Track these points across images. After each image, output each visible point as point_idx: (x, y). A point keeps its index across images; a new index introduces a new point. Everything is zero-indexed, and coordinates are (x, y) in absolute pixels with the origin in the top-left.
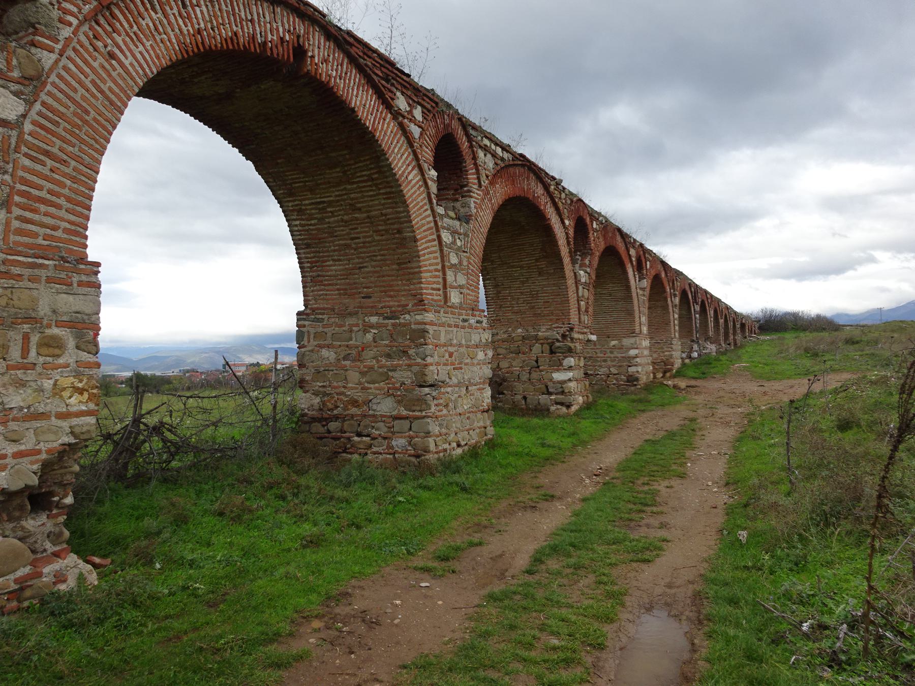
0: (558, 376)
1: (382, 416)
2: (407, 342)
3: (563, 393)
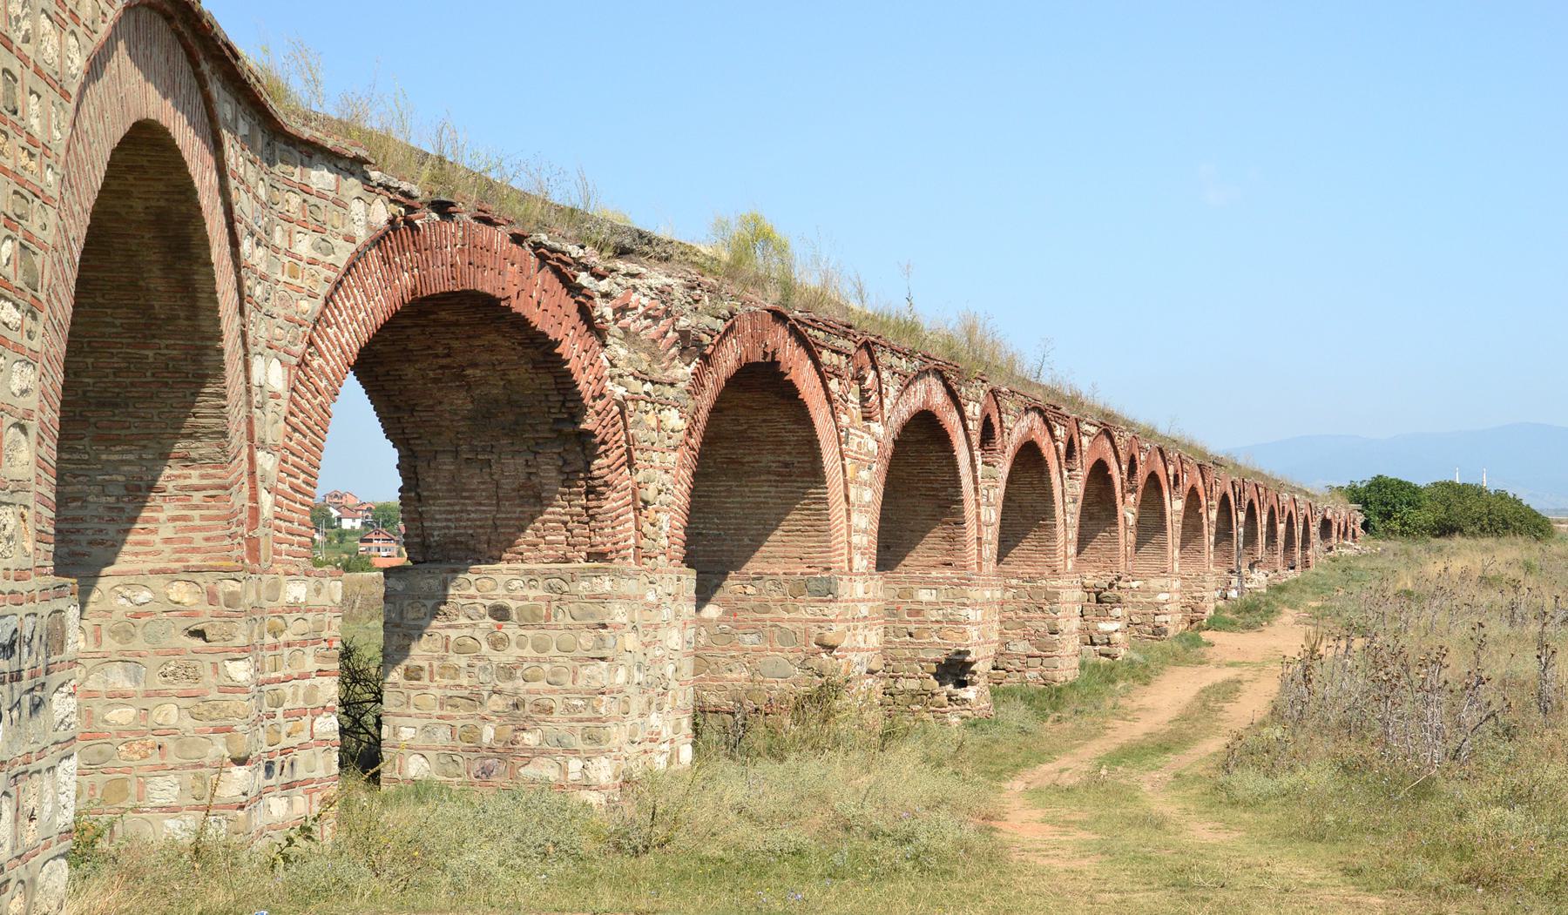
0: (1105, 626)
1: (1017, 655)
2: (1043, 601)
3: (1109, 644)
